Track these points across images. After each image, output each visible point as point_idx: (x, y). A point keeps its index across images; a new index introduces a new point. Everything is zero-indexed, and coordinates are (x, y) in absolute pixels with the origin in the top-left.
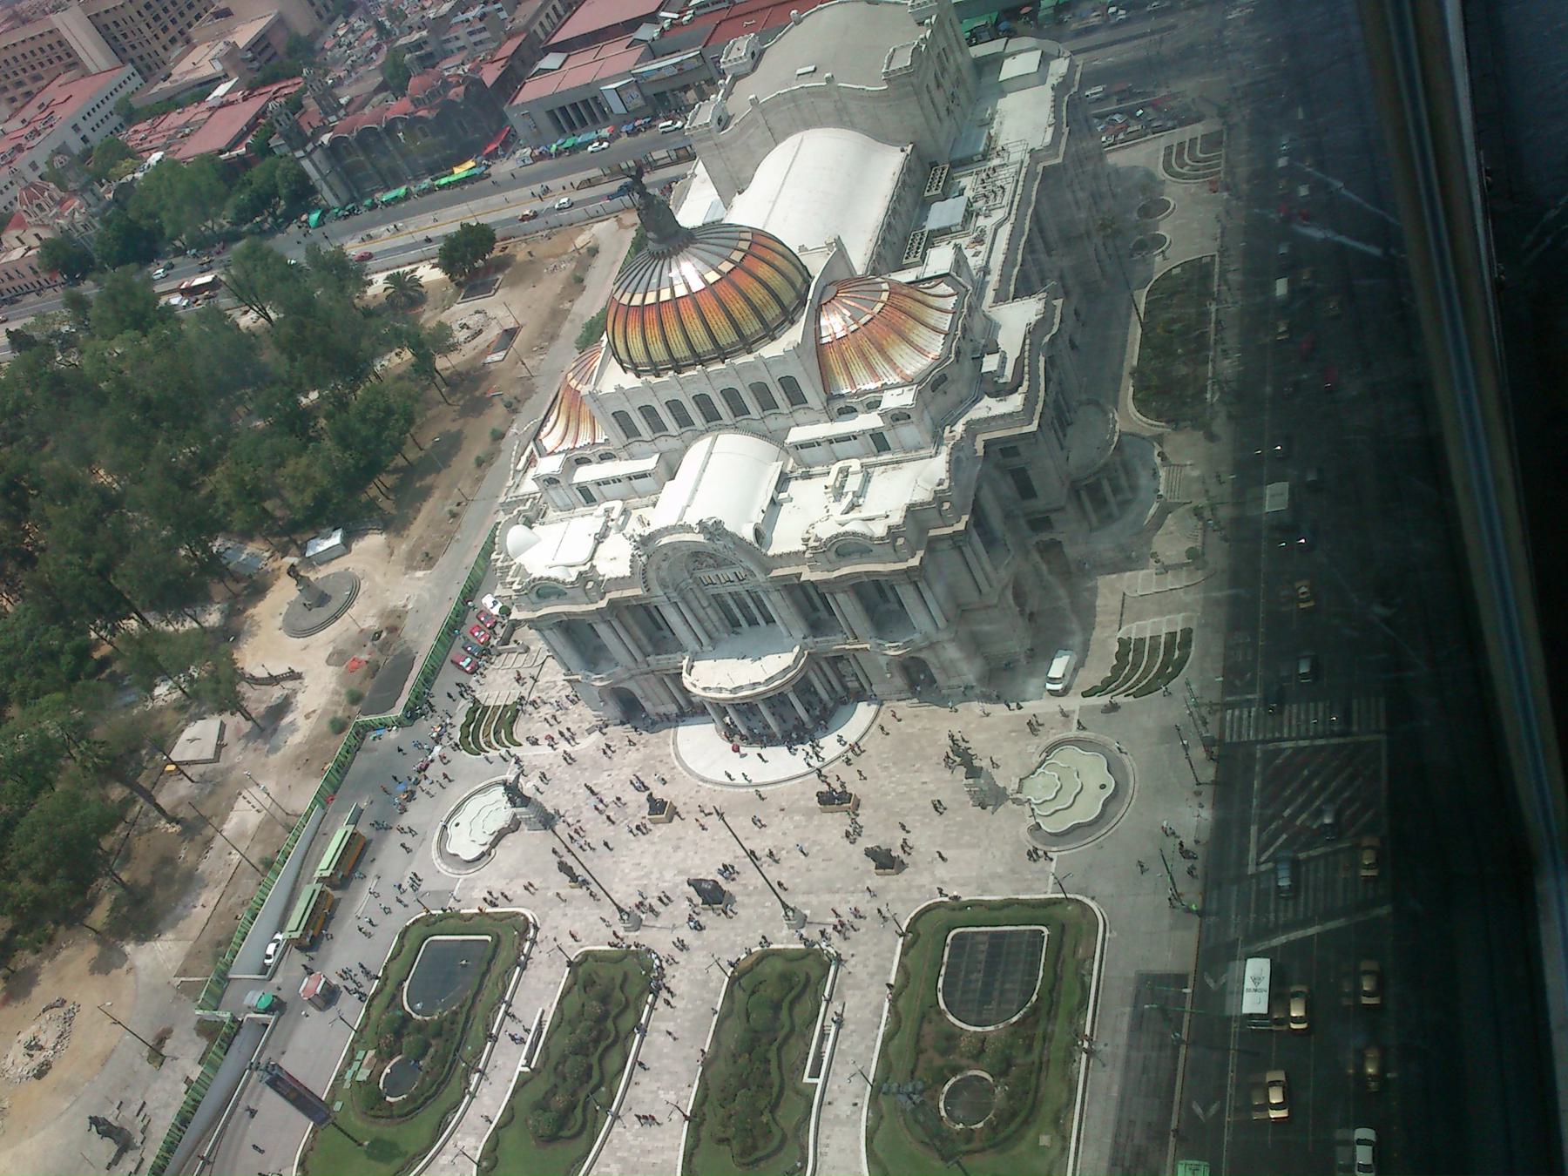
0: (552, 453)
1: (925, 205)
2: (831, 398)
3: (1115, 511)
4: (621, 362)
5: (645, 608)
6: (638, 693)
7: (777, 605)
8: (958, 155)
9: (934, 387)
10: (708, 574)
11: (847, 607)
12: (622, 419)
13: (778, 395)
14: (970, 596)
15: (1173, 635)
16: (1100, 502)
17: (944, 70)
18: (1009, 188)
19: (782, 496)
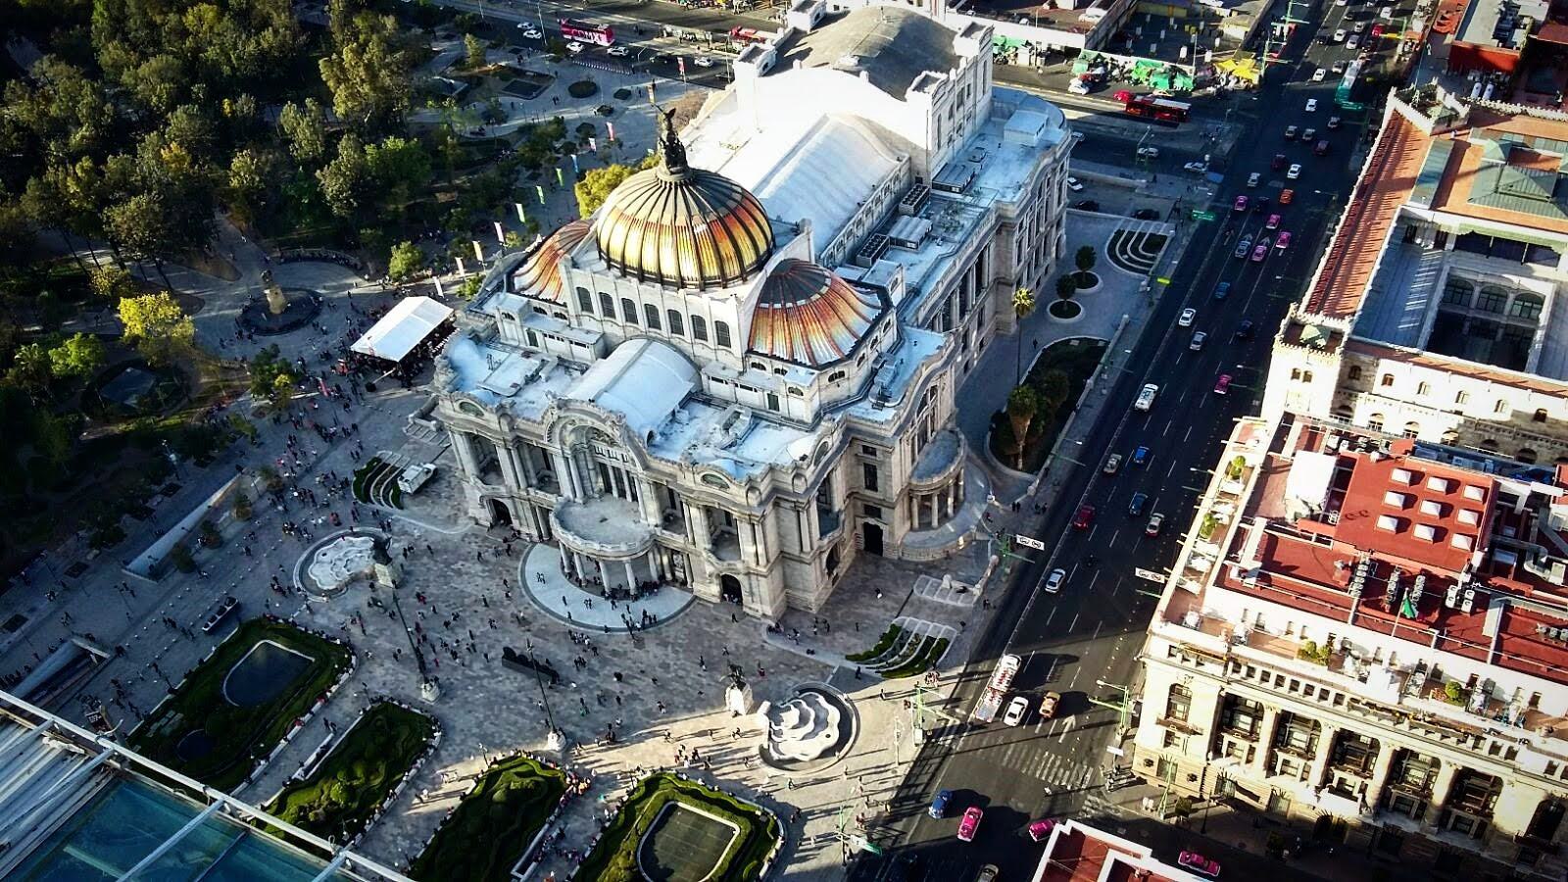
0: (518, 293)
1: (894, 214)
2: (750, 351)
3: (935, 523)
4: (600, 251)
5: (544, 450)
6: (512, 511)
7: (645, 491)
8: (939, 181)
9: (831, 379)
10: (602, 447)
11: (695, 516)
12: (583, 295)
13: (711, 331)
14: (796, 551)
15: (930, 640)
16: (925, 510)
17: (961, 103)
18: (968, 224)
19: (684, 416)
